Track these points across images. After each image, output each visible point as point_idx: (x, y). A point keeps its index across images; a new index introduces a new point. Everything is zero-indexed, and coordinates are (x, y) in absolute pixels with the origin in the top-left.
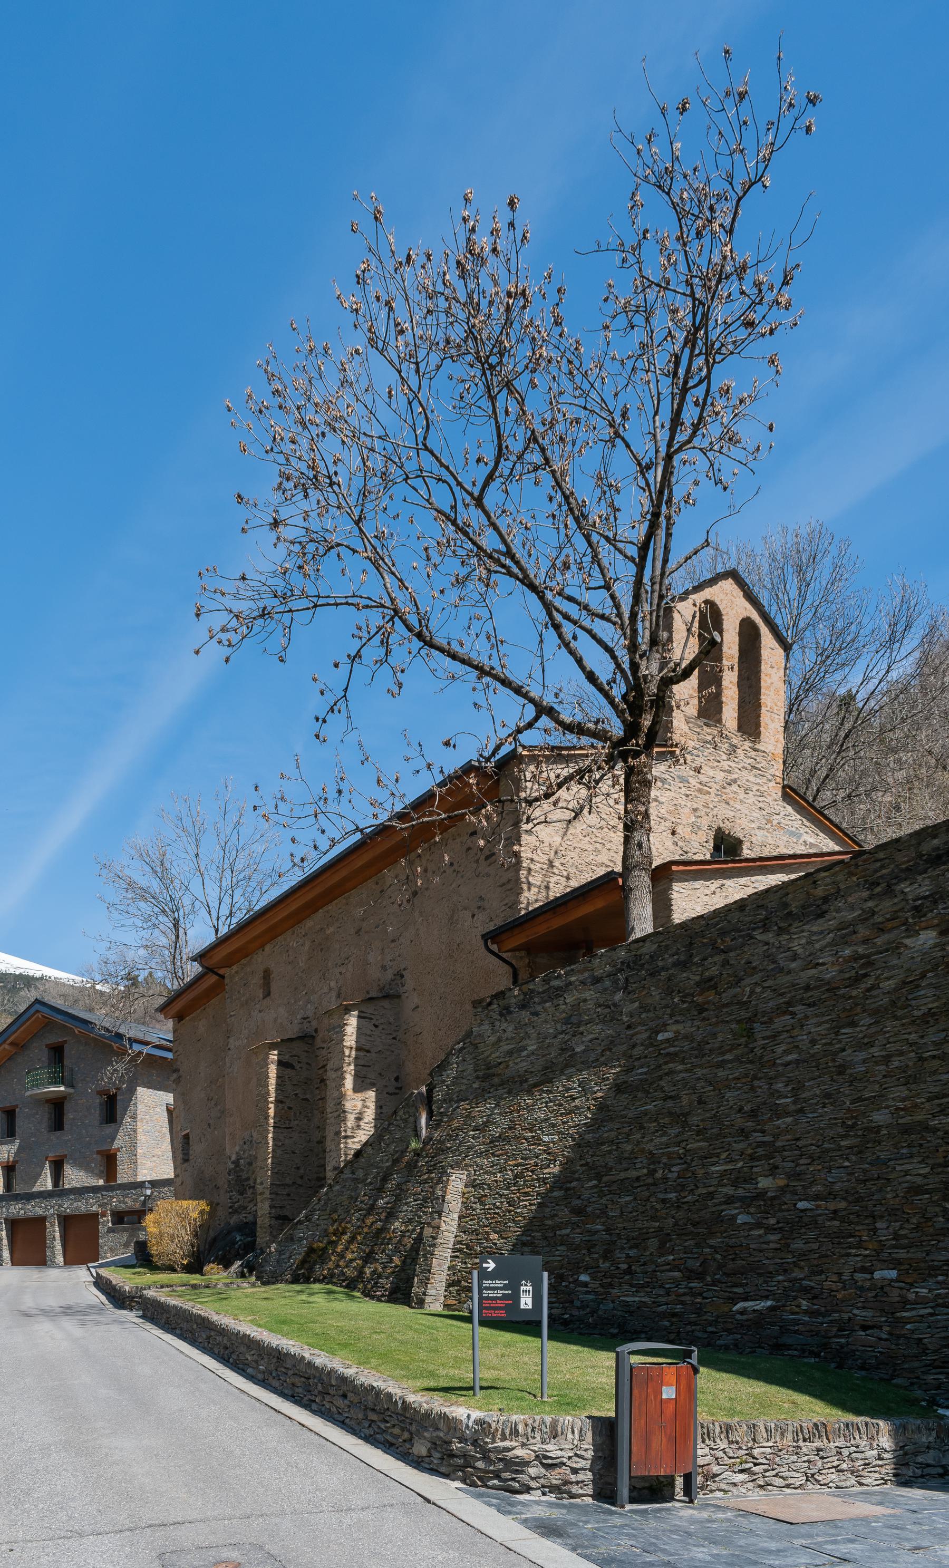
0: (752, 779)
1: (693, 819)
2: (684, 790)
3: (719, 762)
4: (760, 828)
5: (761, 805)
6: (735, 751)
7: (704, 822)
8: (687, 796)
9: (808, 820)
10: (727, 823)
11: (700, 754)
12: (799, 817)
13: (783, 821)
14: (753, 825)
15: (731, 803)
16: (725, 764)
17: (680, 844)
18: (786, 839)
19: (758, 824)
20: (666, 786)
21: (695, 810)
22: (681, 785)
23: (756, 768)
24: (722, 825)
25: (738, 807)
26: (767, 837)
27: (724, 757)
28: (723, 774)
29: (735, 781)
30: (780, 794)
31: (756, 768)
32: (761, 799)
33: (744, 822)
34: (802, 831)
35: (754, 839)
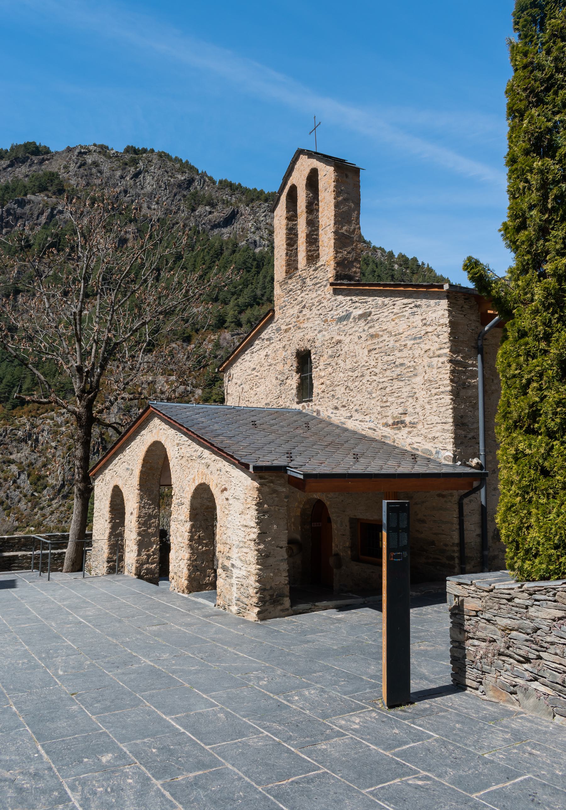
0: (314, 295)
1: (284, 353)
2: (278, 339)
3: (296, 299)
4: (320, 331)
5: (320, 311)
6: (304, 283)
7: (289, 352)
8: (280, 340)
9: (357, 295)
10: (301, 343)
11: (287, 303)
12: (349, 298)
13: (336, 313)
14: (316, 332)
15: (302, 326)
16: (300, 299)
17: (279, 377)
18: (338, 327)
19: (318, 329)
20: (271, 341)
21: (284, 347)
22: (277, 335)
23: (317, 284)
24: (298, 347)
25: (305, 326)
26: (324, 336)
27: (299, 292)
28: (298, 307)
29: (304, 307)
30: (332, 292)
31: (317, 284)
32: (319, 308)
33: (310, 336)
34: (351, 309)
35: (317, 344)
